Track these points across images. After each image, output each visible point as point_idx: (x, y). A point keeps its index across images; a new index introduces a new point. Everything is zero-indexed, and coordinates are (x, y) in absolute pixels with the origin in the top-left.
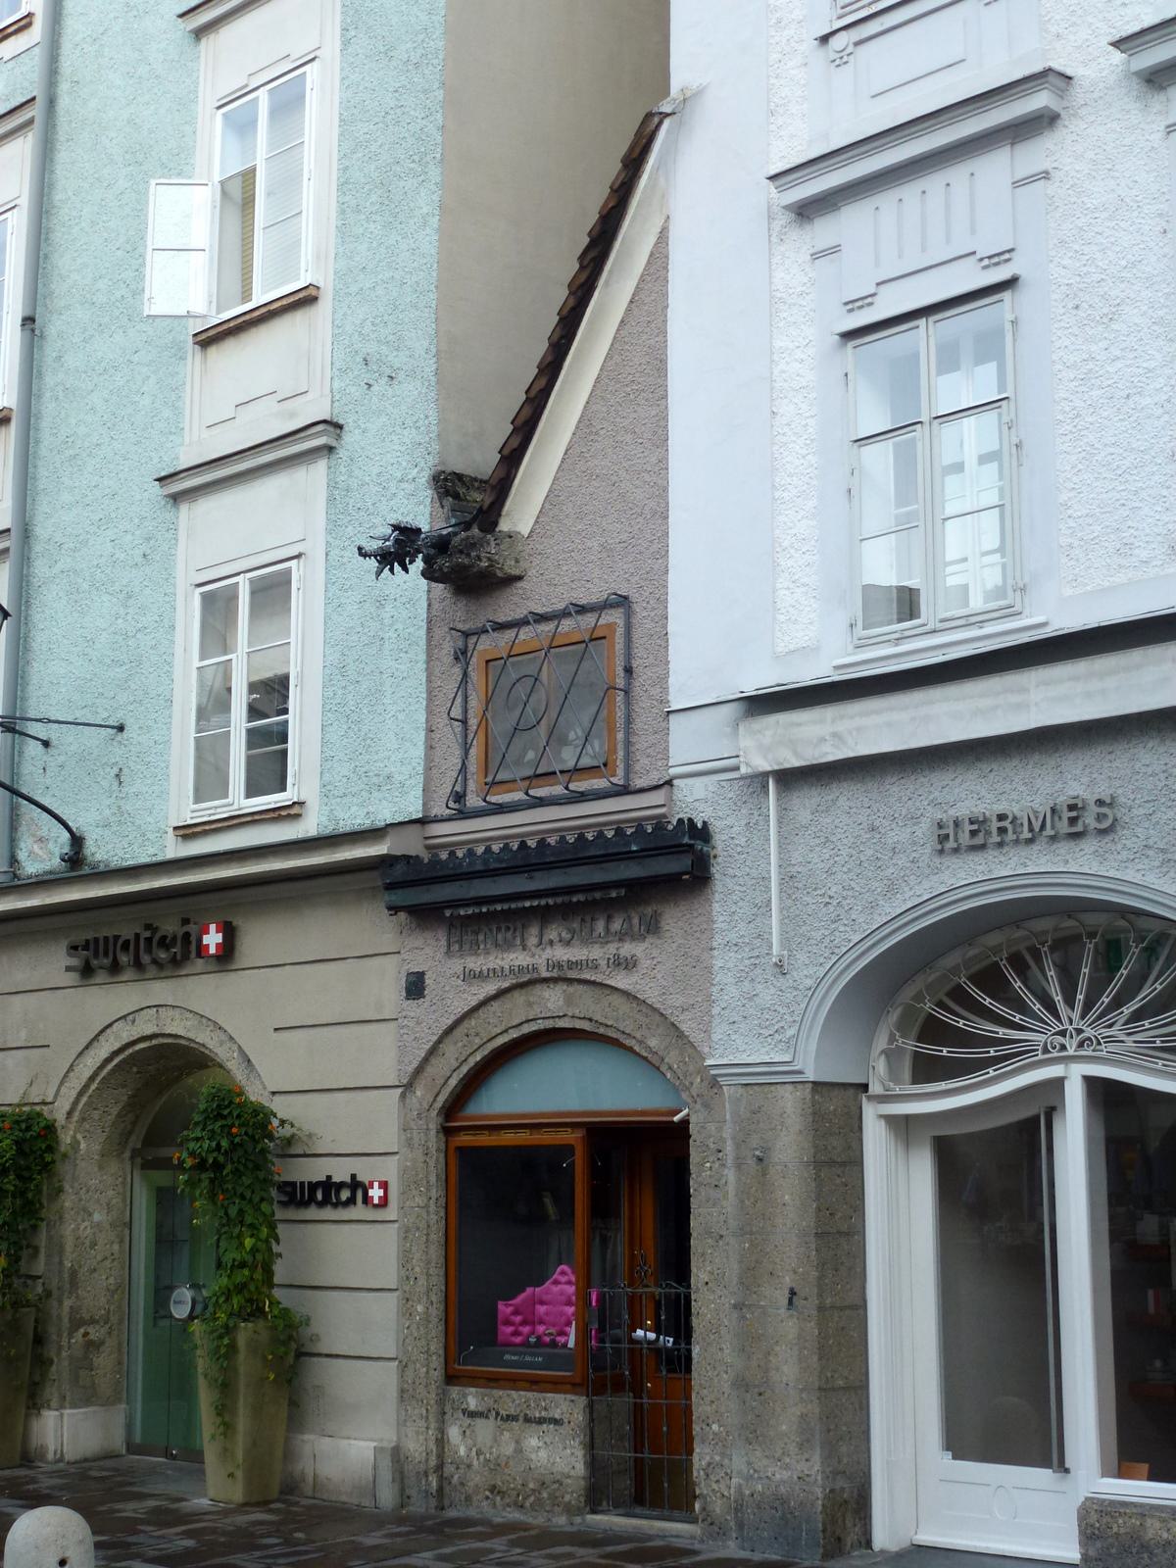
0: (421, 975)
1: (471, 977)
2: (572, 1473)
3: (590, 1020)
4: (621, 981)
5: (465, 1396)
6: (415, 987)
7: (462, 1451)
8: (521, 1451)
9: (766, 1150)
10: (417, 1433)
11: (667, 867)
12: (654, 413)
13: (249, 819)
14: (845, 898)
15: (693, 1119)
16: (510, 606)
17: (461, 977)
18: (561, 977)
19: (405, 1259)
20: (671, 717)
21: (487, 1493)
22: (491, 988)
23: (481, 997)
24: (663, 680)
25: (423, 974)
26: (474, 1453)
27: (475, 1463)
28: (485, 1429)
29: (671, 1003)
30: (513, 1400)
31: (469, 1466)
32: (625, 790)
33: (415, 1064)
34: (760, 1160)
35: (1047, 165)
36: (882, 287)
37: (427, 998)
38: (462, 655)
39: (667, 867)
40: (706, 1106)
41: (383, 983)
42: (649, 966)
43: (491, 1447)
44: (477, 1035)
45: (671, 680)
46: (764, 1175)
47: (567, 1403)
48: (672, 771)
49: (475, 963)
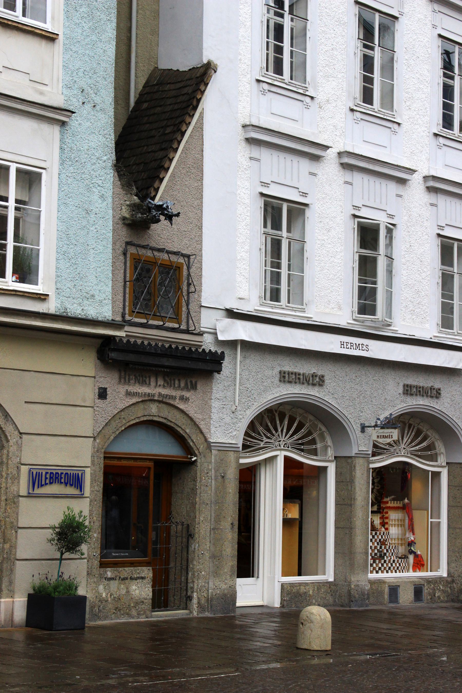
0: (105, 389)
1: (128, 394)
2: (148, 597)
3: (165, 419)
4: (182, 406)
5: (106, 572)
6: (103, 394)
7: (104, 595)
8: (129, 592)
9: (224, 473)
10: (92, 590)
11: (199, 366)
12: (196, 185)
13: (22, 294)
14: (252, 390)
15: (199, 461)
17: (123, 395)
18: (163, 401)
20: (202, 309)
21: (114, 611)
22: (134, 400)
23: (131, 403)
25: (106, 388)
26: (109, 595)
27: (109, 599)
28: (114, 585)
29: (197, 417)
30: (126, 571)
31: (107, 601)
32: (187, 332)
33: (100, 429)
34: (223, 477)
35: (316, 172)
36: (272, 184)
37: (107, 400)
40: (204, 456)
41: (88, 392)
43: (116, 592)
44: (124, 418)
45: (203, 294)
46: (224, 482)
47: (147, 570)
48: (202, 329)
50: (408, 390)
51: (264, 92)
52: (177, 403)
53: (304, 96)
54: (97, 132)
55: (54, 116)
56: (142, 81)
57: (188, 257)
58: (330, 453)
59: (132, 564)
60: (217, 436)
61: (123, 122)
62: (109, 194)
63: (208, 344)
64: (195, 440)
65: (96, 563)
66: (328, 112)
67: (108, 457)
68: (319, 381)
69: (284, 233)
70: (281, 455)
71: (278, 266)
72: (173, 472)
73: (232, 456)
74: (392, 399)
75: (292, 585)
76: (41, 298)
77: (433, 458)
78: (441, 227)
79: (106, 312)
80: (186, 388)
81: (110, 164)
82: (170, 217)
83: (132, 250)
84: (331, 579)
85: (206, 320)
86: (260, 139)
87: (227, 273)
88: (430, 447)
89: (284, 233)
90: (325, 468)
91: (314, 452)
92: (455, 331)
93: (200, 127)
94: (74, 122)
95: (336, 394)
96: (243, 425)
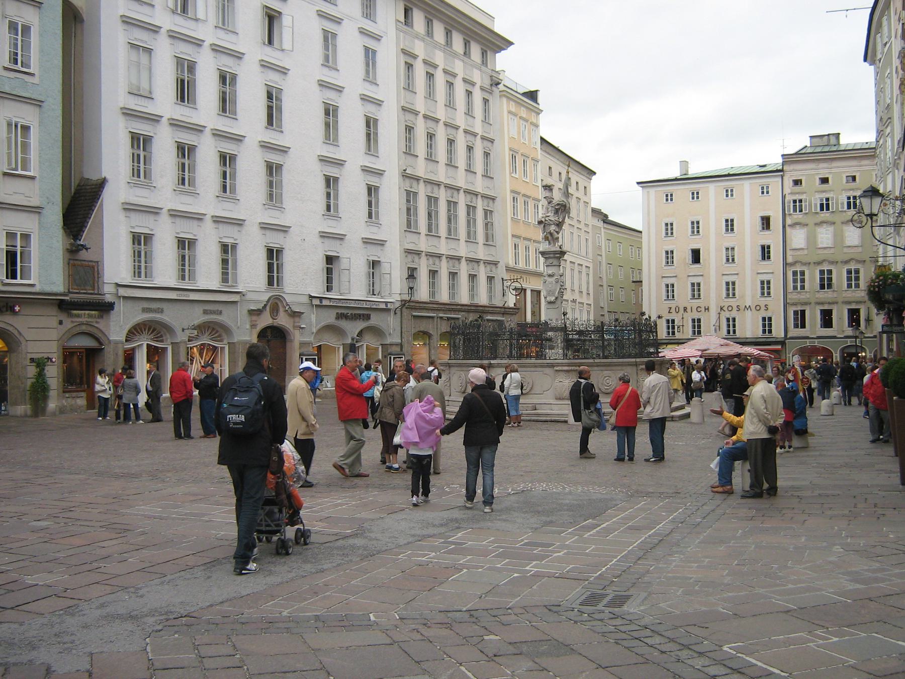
6: (61, 323)
11: (106, 308)
28: (69, 400)
29: (104, 329)
30: (74, 394)
39: (106, 308)
41: (54, 322)
50: (205, 312)
51: (131, 187)
53: (150, 187)
54: (55, 215)
55: (36, 210)
56: (77, 182)
58: (169, 341)
59: (77, 391)
60: (113, 337)
61: (68, 202)
62: (61, 236)
63: (109, 298)
64: (103, 339)
65: (61, 391)
66: (164, 192)
67: (65, 349)
68: (161, 311)
69: (143, 246)
70: (145, 344)
71: (140, 262)
72: (92, 355)
73: (120, 345)
74: (197, 316)
76: (32, 285)
77: (221, 341)
78: (221, 238)
82: (87, 249)
83: (72, 262)
86: (130, 208)
87: (116, 268)
88: (220, 336)
89: (143, 246)
91: (162, 341)
92: (230, 284)
93: (102, 205)
94: (44, 211)
95: (169, 316)
96: (126, 331)
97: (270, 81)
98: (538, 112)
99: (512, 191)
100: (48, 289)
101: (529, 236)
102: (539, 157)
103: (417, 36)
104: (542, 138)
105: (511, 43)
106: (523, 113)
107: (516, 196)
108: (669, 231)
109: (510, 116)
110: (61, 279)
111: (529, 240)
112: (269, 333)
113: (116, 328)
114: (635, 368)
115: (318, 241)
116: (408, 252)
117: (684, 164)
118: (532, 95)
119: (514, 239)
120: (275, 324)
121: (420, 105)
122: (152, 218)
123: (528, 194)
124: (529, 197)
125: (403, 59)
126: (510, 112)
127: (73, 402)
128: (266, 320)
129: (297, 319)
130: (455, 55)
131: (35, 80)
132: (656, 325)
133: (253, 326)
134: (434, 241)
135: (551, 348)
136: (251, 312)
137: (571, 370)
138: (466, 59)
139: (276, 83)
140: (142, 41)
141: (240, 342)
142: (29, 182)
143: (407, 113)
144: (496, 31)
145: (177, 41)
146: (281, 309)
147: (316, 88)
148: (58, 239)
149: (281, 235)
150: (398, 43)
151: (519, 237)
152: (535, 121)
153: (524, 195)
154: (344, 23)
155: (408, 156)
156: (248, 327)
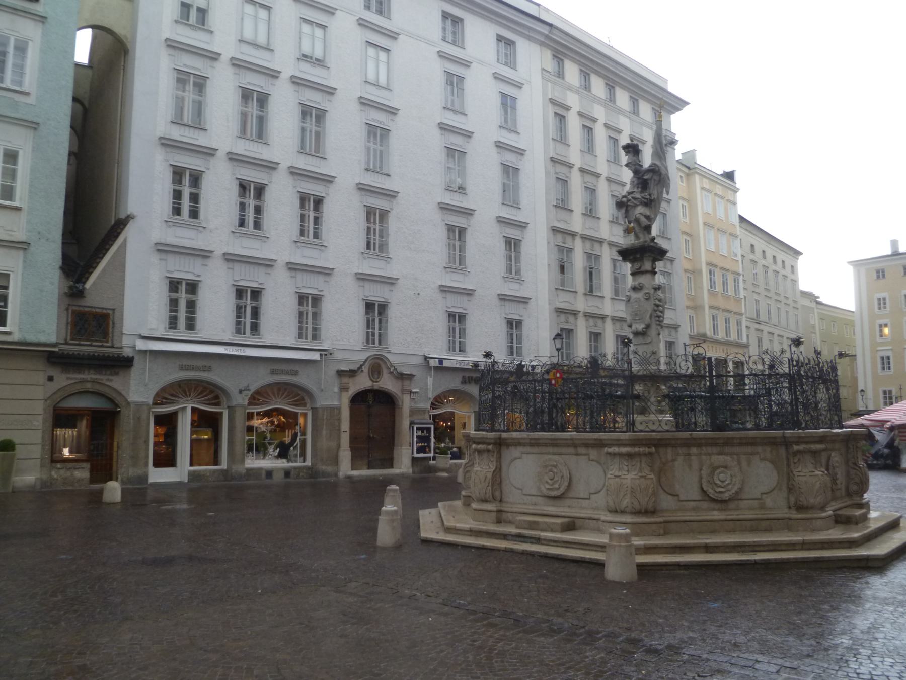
1: (68, 379)
6: (51, 379)
16: (83, 302)
17: (63, 380)
18: (93, 381)
19: (43, 437)
22: (73, 381)
24: (122, 327)
28: (62, 472)
32: (112, 347)
38: (67, 310)
39: (122, 363)
41: (41, 377)
42: (116, 382)
49: (69, 376)
50: (273, 372)
51: (170, 226)
52: (104, 382)
54: (50, 252)
55: (22, 246)
57: (113, 310)
63: (127, 352)
64: (118, 400)
65: (48, 461)
70: (189, 407)
75: (195, 471)
77: (304, 405)
79: (53, 339)
80: (111, 374)
81: (58, 267)
84: (225, 468)
85: (126, 341)
86: (164, 250)
90: (221, 413)
94: (32, 249)
97: (373, 120)
98: (735, 191)
99: (708, 264)
100: (31, 338)
101: (729, 308)
102: (738, 233)
103: (570, 88)
104: (740, 217)
105: (687, 103)
106: (719, 190)
107: (712, 268)
108: (882, 306)
109: (704, 193)
110: (55, 327)
111: (730, 312)
112: (370, 398)
113: (138, 390)
114: (782, 451)
115: (439, 296)
116: (560, 311)
117: (894, 243)
118: (730, 176)
119: (713, 311)
120: (376, 388)
121: (575, 157)
122: (199, 262)
123: (727, 267)
124: (728, 270)
125: (551, 110)
126: (703, 189)
127: (69, 474)
128: (363, 382)
129: (407, 383)
130: (620, 111)
131: (31, 100)
132: (834, 369)
133: (344, 389)
134: (597, 302)
135: (643, 411)
136: (340, 373)
137: (639, 455)
138: (634, 117)
139: (383, 123)
140: (193, 68)
141: (325, 408)
142: (12, 215)
143: (557, 165)
144: (670, 89)
145: (242, 70)
146: (385, 371)
147: (437, 132)
148: (52, 281)
149: (386, 288)
150: (544, 94)
151: (718, 309)
152: (731, 199)
153: (722, 268)
154: (474, 65)
155: (559, 211)
156: (336, 390)
